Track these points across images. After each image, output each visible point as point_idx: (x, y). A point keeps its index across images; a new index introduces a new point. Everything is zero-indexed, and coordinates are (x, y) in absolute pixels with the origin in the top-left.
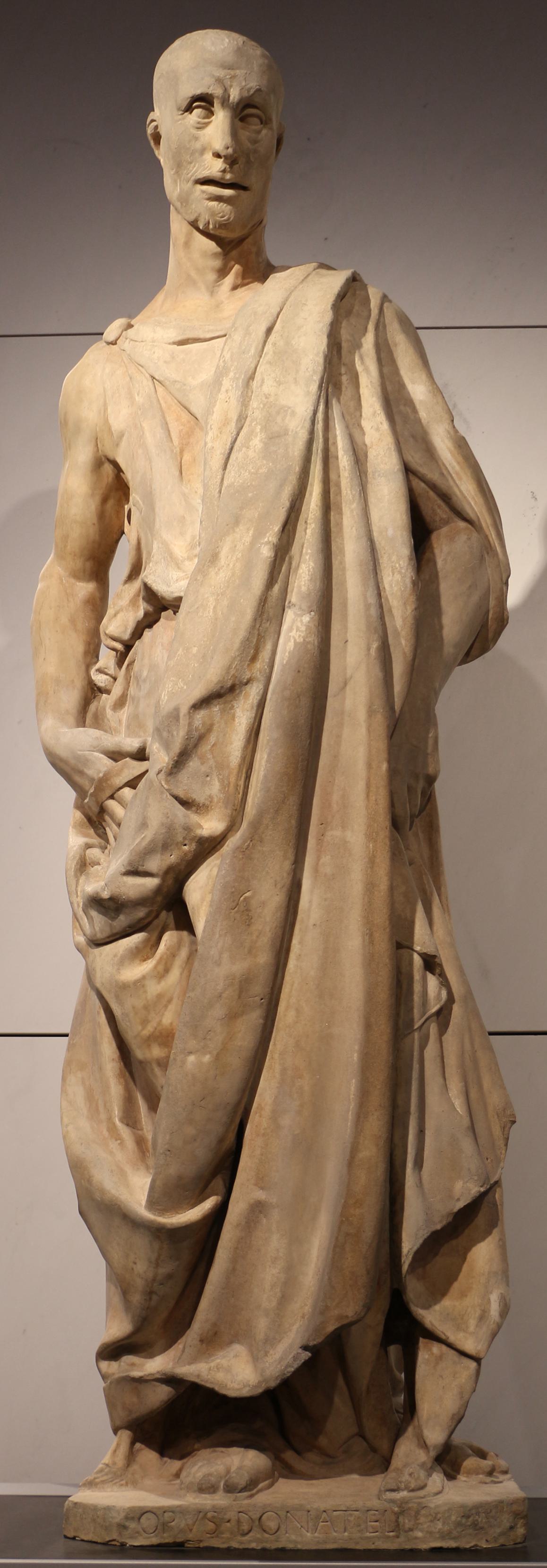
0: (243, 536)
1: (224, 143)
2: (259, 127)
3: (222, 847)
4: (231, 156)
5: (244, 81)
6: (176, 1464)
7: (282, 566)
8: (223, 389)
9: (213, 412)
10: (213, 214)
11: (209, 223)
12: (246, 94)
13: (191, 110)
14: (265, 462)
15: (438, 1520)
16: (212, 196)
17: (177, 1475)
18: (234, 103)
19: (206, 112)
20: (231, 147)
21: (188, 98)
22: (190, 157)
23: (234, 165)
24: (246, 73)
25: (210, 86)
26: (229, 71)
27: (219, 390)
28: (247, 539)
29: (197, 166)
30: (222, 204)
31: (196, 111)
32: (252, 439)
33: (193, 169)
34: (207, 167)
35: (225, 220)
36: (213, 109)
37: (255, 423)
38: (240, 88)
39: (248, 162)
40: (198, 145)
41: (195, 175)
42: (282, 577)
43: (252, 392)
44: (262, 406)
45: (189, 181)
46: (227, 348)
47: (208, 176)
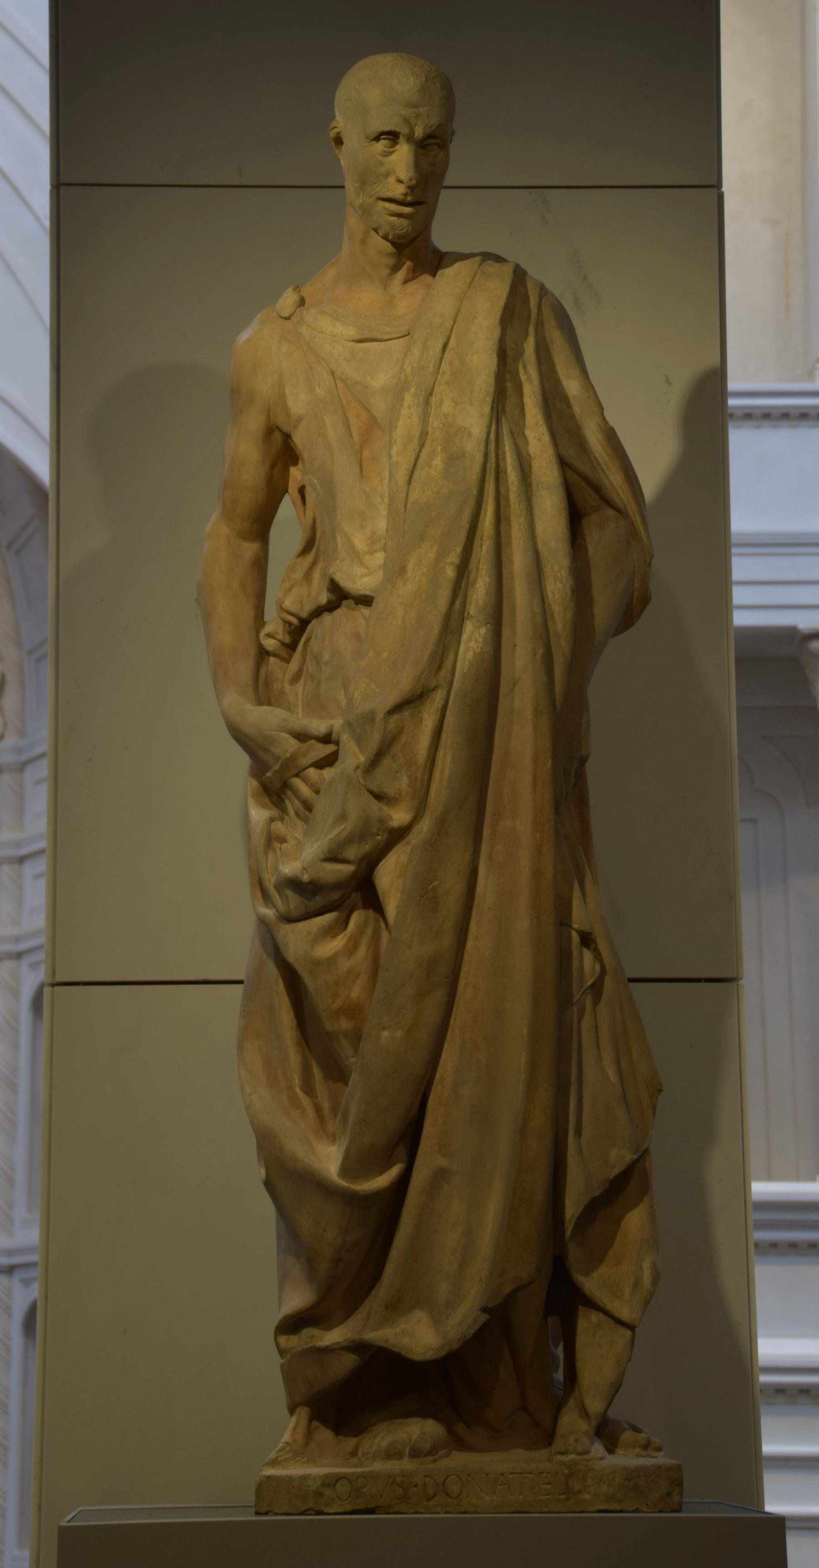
0: (428, 552)
3: (407, 835)
6: (352, 1442)
7: (462, 581)
8: (406, 404)
9: (397, 427)
15: (604, 1483)
17: (354, 1453)
27: (402, 404)
28: (432, 554)
37: (436, 443)
42: (462, 590)
44: (441, 426)
46: (407, 361)
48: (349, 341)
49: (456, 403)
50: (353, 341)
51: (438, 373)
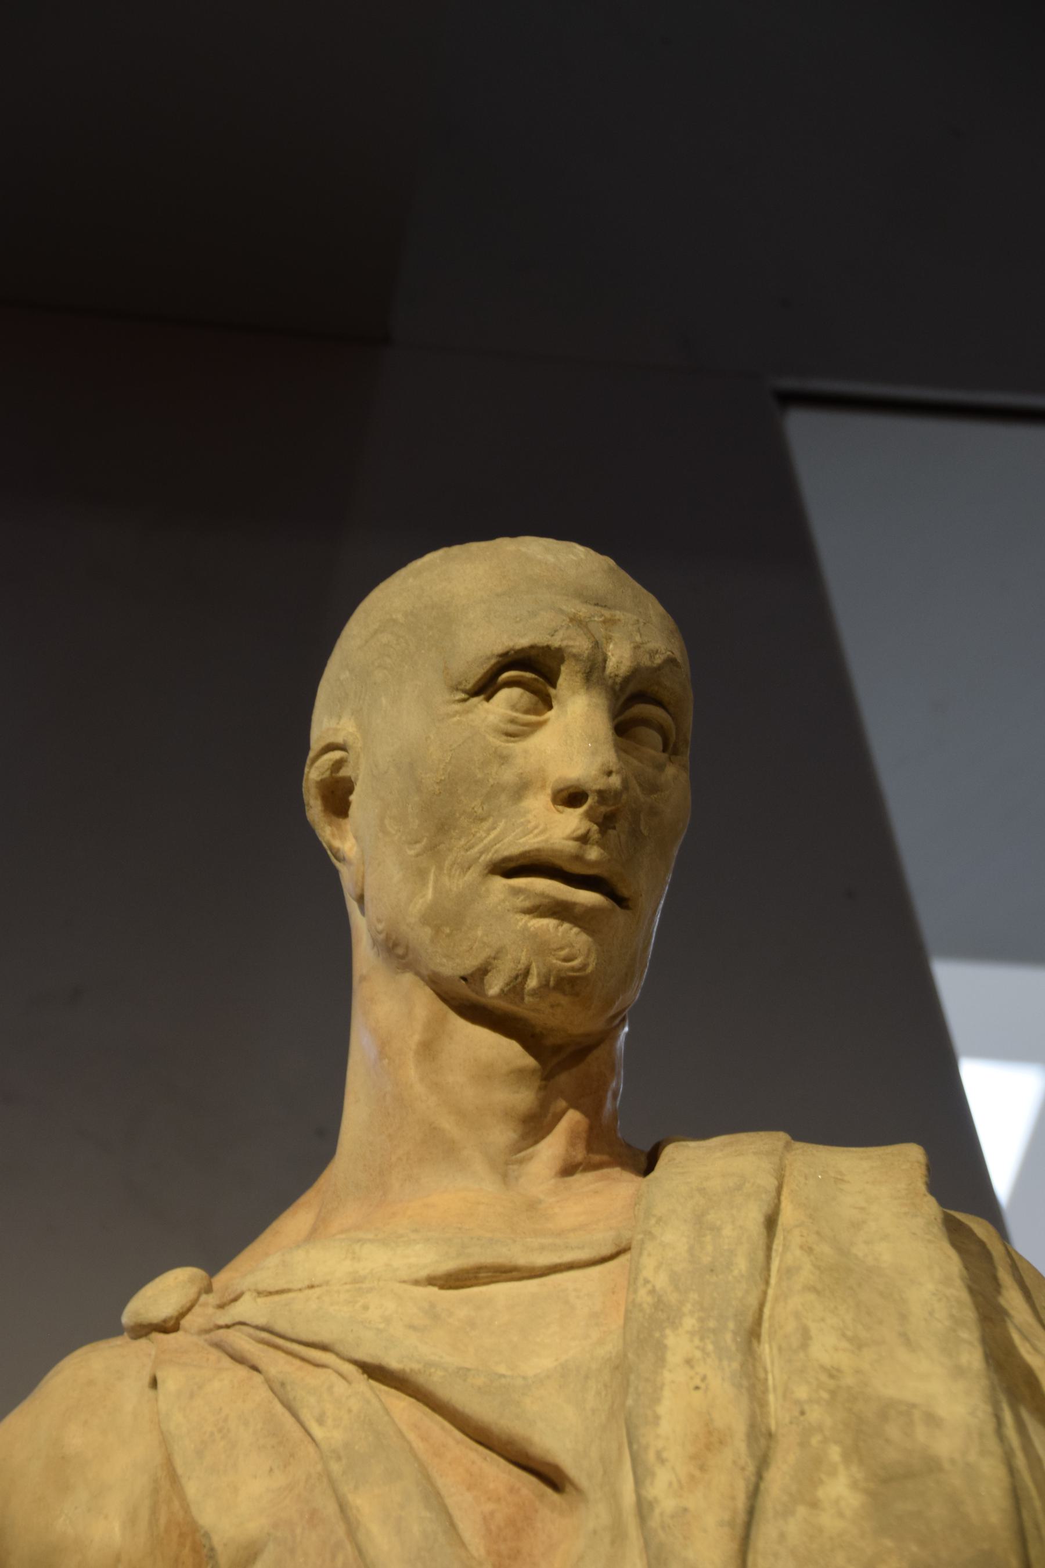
1: (599, 760)
2: (663, 757)
4: (617, 794)
5: (638, 634)
8: (674, 1358)
9: (657, 1418)
10: (542, 947)
11: (527, 973)
12: (645, 661)
13: (489, 692)
14: (889, 1543)
16: (546, 901)
18: (616, 676)
19: (534, 698)
20: (618, 772)
21: (489, 658)
22: (483, 803)
23: (610, 828)
24: (638, 621)
25: (556, 631)
26: (597, 608)
29: (502, 824)
30: (566, 925)
31: (505, 695)
32: (821, 1482)
33: (488, 834)
34: (536, 827)
35: (573, 969)
36: (552, 691)
38: (632, 645)
39: (635, 833)
40: (508, 775)
41: (493, 850)
43: (766, 1372)
44: (825, 1395)
45: (469, 868)
47: (538, 850)
48: (417, 1283)
49: (858, 1345)
50: (432, 1281)
51: (767, 1283)
